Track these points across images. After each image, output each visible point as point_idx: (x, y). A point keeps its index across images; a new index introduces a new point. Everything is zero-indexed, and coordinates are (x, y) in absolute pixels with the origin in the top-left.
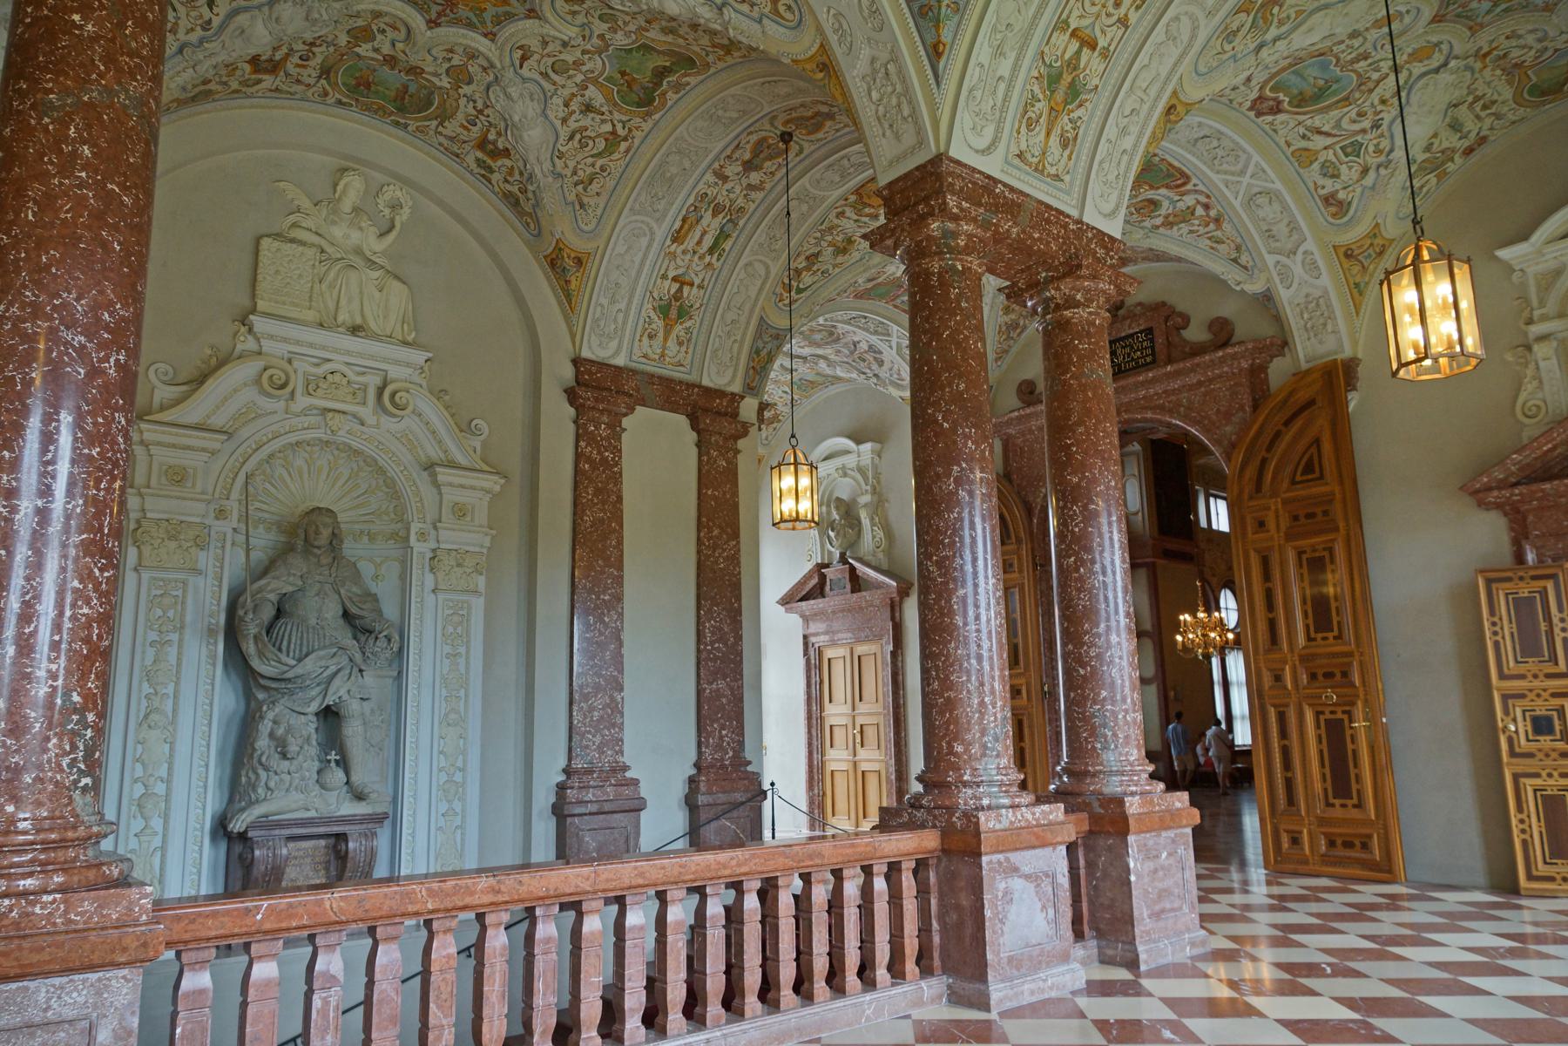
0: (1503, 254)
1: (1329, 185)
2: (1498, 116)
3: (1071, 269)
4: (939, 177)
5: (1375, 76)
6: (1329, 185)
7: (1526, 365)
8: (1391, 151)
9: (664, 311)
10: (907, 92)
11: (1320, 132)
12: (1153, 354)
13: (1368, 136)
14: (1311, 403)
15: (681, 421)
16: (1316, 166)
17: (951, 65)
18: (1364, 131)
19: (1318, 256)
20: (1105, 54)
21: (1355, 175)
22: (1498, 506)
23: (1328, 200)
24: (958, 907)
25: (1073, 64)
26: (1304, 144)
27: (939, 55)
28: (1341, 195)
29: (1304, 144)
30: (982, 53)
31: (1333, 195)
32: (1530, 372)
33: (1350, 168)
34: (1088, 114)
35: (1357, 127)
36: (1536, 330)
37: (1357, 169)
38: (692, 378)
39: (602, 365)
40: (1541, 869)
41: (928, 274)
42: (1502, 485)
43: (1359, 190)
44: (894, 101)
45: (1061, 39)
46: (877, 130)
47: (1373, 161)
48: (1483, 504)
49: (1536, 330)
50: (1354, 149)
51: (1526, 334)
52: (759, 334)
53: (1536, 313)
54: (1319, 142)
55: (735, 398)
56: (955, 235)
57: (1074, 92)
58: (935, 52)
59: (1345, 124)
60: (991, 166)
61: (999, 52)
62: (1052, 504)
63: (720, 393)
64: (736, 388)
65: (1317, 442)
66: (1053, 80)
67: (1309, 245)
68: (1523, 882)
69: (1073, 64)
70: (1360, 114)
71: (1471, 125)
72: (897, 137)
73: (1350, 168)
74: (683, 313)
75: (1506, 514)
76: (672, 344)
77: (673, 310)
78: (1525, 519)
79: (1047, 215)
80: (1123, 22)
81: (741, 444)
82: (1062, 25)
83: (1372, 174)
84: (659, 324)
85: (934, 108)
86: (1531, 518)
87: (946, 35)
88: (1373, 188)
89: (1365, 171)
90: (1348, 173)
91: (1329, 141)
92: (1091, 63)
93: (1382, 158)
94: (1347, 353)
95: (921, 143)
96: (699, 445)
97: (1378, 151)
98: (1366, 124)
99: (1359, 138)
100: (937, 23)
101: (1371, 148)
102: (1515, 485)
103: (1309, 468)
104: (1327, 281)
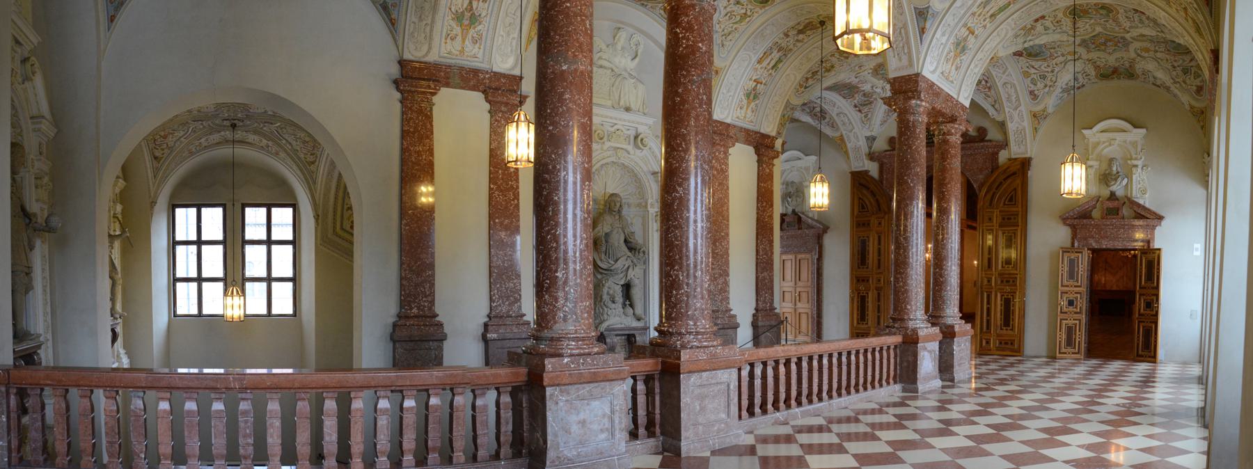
3: (953, 120)
4: (917, 82)
9: (748, 95)
10: (908, 43)
15: (751, 150)
17: (927, 37)
20: (976, 37)
25: (965, 39)
30: (938, 35)
34: (966, 58)
38: (756, 129)
39: (722, 123)
41: (908, 121)
45: (964, 30)
52: (786, 107)
55: (774, 139)
56: (920, 106)
57: (964, 49)
58: (922, 31)
60: (933, 78)
61: (943, 34)
62: (919, 207)
63: (768, 136)
64: (773, 134)
66: (958, 44)
69: (965, 39)
72: (900, 59)
74: (756, 97)
76: (749, 111)
77: (752, 95)
79: (949, 98)
80: (985, 27)
81: (775, 161)
82: (965, 25)
84: (745, 101)
85: (918, 53)
87: (928, 25)
92: (971, 39)
95: (911, 64)
96: (758, 161)
100: (925, 20)
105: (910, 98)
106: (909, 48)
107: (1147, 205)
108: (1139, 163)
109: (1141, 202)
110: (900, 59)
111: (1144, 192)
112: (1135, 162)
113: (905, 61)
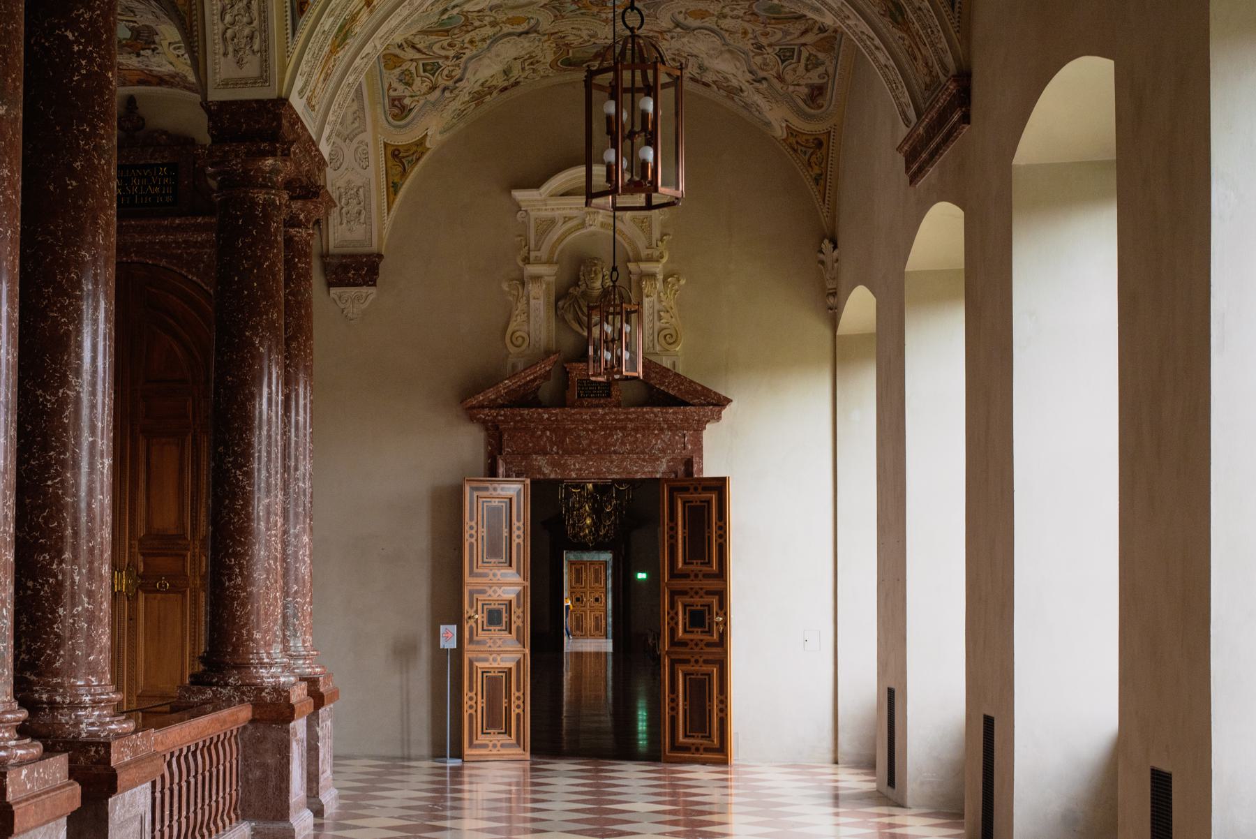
0: (519, 195)
1: (401, 90)
2: (534, 71)
4: (278, 118)
5: (477, 23)
6: (401, 90)
7: (518, 299)
8: (460, 80)
11: (414, 47)
13: (448, 63)
16: (397, 71)
17: (306, 22)
18: (447, 58)
19: (371, 150)
21: (424, 88)
26: (398, 51)
27: (302, 12)
28: (407, 101)
29: (398, 51)
31: (400, 99)
32: (521, 305)
33: (423, 82)
35: (443, 53)
36: (531, 269)
37: (428, 83)
42: (493, 405)
43: (422, 102)
44: (247, 31)
46: (220, 48)
47: (442, 82)
48: (472, 419)
49: (531, 269)
50: (432, 69)
51: (522, 270)
53: (533, 254)
54: (411, 54)
56: (278, 172)
59: (436, 48)
67: (367, 136)
70: (450, 45)
71: (515, 73)
72: (239, 63)
73: (423, 82)
75: (487, 429)
78: (501, 436)
83: (438, 92)
85: (286, 54)
86: (506, 436)
88: (434, 104)
89: (433, 88)
90: (419, 85)
91: (418, 56)
93: (451, 83)
95: (263, 78)
97: (450, 76)
98: (451, 53)
99: (440, 62)
101: (446, 72)
102: (502, 406)
104: (374, 173)
105: (265, 154)
106: (265, 41)
108: (658, 268)
112: (646, 267)
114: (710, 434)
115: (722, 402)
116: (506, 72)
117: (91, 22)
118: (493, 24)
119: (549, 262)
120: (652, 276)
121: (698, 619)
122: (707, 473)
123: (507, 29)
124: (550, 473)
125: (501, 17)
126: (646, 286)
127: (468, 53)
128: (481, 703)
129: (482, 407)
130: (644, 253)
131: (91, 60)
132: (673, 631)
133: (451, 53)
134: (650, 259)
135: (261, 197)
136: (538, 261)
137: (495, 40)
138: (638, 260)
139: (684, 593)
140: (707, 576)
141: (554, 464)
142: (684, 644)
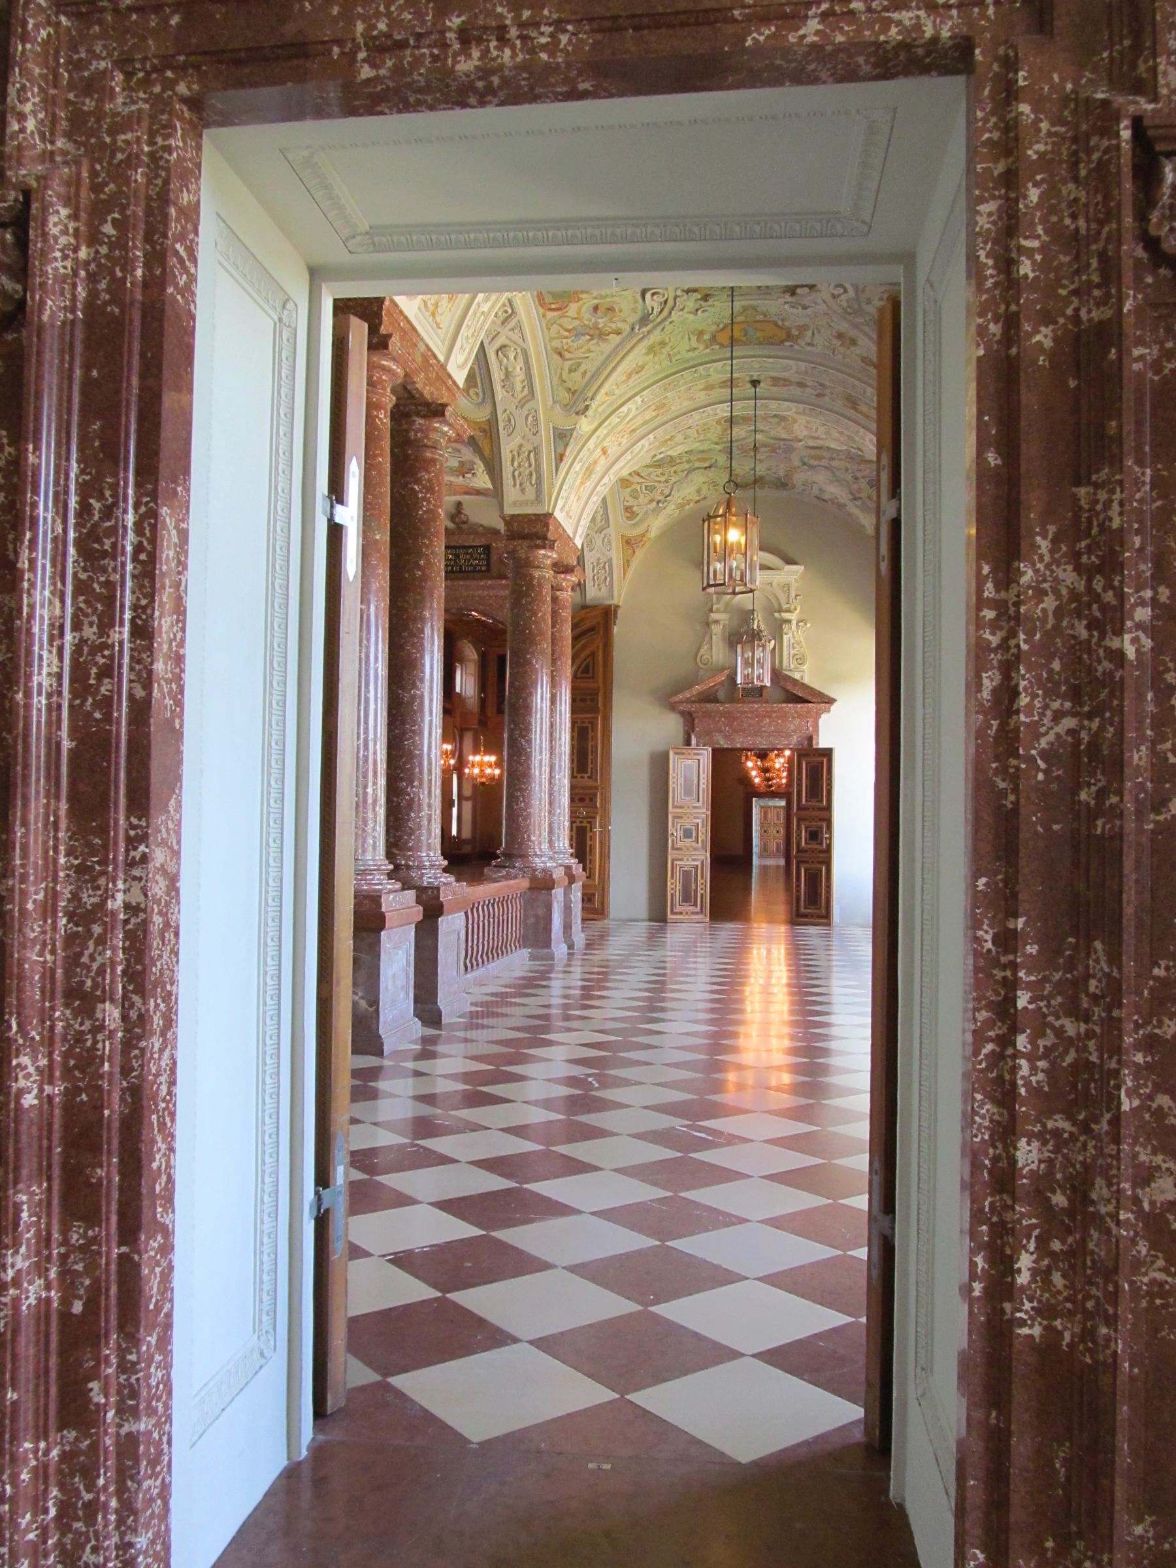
1: (631, 502)
4: (547, 525)
12: (488, 565)
14: (592, 629)
17: (564, 467)
21: (646, 500)
22: (682, 713)
23: (628, 509)
24: (536, 916)
36: (714, 616)
40: (678, 909)
42: (688, 701)
46: (511, 481)
48: (672, 707)
49: (714, 616)
50: (650, 489)
58: (560, 458)
65: (593, 654)
68: (669, 916)
71: (704, 491)
72: (523, 491)
85: (552, 486)
89: (652, 501)
94: (615, 602)
98: (663, 479)
100: (567, 445)
103: (586, 670)
106: (539, 478)
107: (806, 681)
108: (793, 617)
109: (797, 676)
110: (523, 491)
111: (801, 660)
112: (786, 616)
113: (530, 494)
114: (824, 720)
115: (830, 701)
116: (698, 491)
117: (429, 480)
118: (688, 462)
119: (725, 611)
120: (789, 621)
121: (814, 836)
122: (821, 746)
123: (697, 465)
124: (724, 744)
125: (693, 458)
126: (785, 627)
127: (673, 480)
128: (679, 887)
129: (681, 702)
130: (785, 606)
131: (429, 502)
132: (799, 843)
133: (663, 479)
134: (788, 611)
135: (537, 574)
136: (718, 611)
137: (690, 471)
138: (780, 611)
139: (804, 819)
140: (821, 809)
141: (726, 737)
142: (805, 851)
